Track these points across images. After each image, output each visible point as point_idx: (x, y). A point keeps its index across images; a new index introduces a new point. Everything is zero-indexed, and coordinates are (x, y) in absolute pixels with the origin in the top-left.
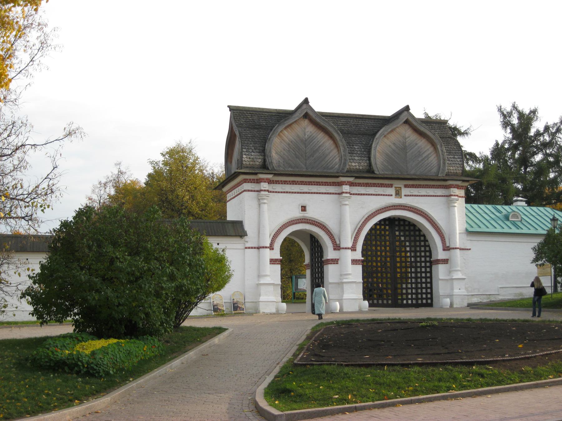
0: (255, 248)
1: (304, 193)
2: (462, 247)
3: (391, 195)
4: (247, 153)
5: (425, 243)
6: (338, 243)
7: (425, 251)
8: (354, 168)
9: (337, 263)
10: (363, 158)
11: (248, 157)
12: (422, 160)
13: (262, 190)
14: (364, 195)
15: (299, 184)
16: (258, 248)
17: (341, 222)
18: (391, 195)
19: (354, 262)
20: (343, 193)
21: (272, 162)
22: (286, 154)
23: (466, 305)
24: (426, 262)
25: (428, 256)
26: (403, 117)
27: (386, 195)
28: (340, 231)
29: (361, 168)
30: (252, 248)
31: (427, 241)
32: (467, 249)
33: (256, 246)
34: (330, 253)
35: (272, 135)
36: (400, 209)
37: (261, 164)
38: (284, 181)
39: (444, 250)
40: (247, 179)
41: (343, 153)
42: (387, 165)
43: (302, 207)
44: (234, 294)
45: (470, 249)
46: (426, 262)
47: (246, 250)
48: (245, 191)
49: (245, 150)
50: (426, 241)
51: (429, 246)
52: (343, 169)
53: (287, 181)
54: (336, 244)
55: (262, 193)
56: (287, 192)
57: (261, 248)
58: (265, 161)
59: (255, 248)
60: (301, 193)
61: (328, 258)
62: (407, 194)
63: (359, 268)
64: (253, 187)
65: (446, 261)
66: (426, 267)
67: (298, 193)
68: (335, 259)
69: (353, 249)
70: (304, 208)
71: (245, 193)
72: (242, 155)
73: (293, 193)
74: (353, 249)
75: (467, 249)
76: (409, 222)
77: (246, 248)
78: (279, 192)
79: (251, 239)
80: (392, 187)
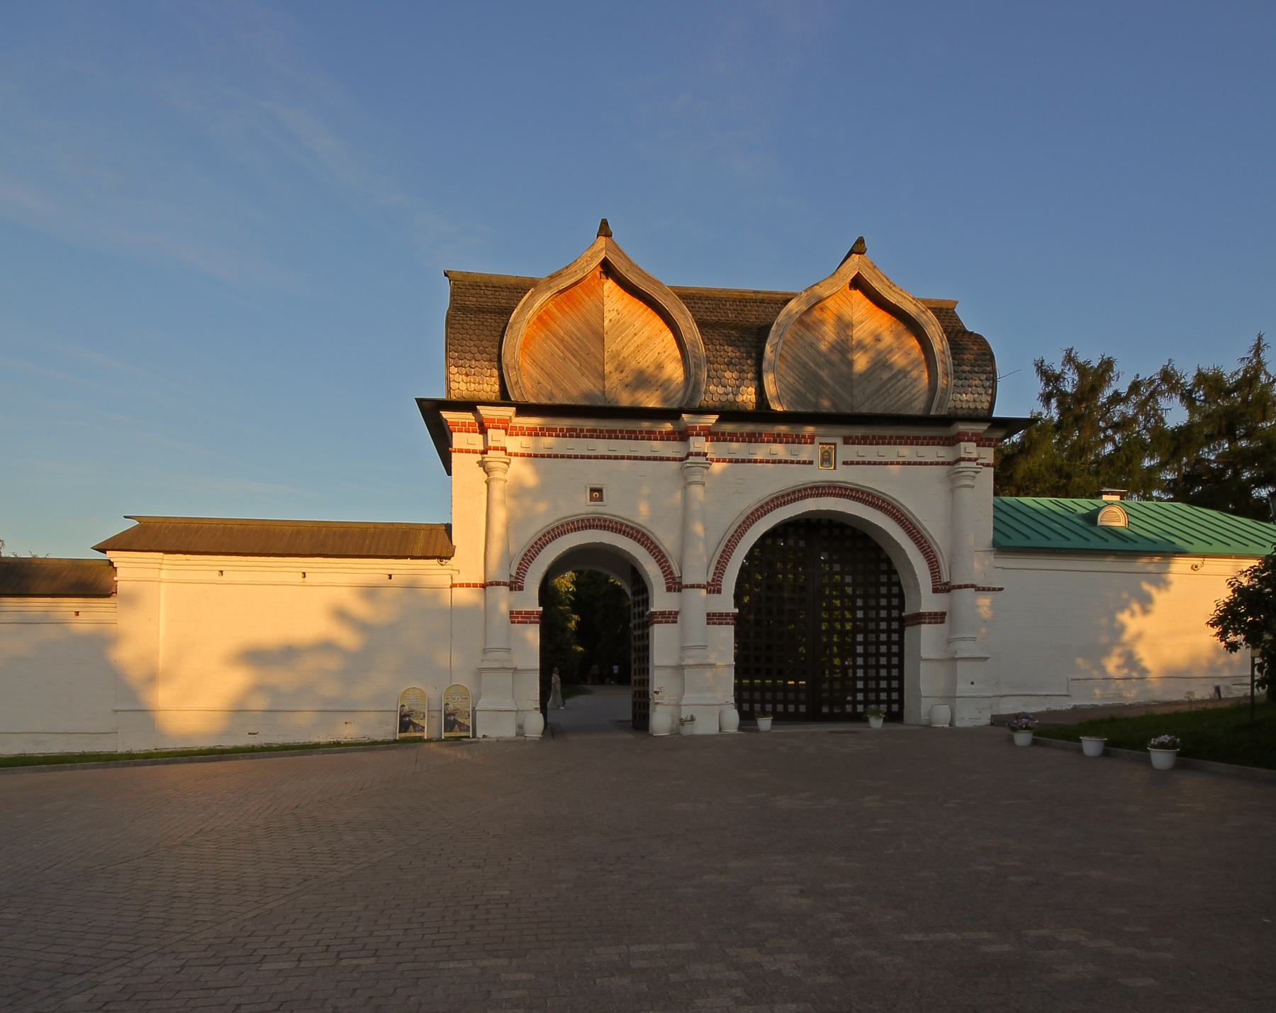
2: (981, 585)
3: (811, 463)
6: (677, 574)
7: (889, 596)
18: (811, 463)
19: (714, 618)
24: (889, 620)
25: (895, 607)
31: (895, 572)
32: (994, 589)
34: (661, 600)
39: (935, 591)
42: (803, 390)
43: (593, 490)
44: (404, 695)
46: (889, 620)
50: (892, 571)
54: (674, 579)
62: (849, 460)
63: (727, 634)
65: (938, 618)
66: (889, 631)
67: (583, 457)
68: (670, 613)
69: (714, 587)
70: (597, 493)
74: (714, 587)
75: (994, 589)
76: (854, 530)
80: (812, 443)
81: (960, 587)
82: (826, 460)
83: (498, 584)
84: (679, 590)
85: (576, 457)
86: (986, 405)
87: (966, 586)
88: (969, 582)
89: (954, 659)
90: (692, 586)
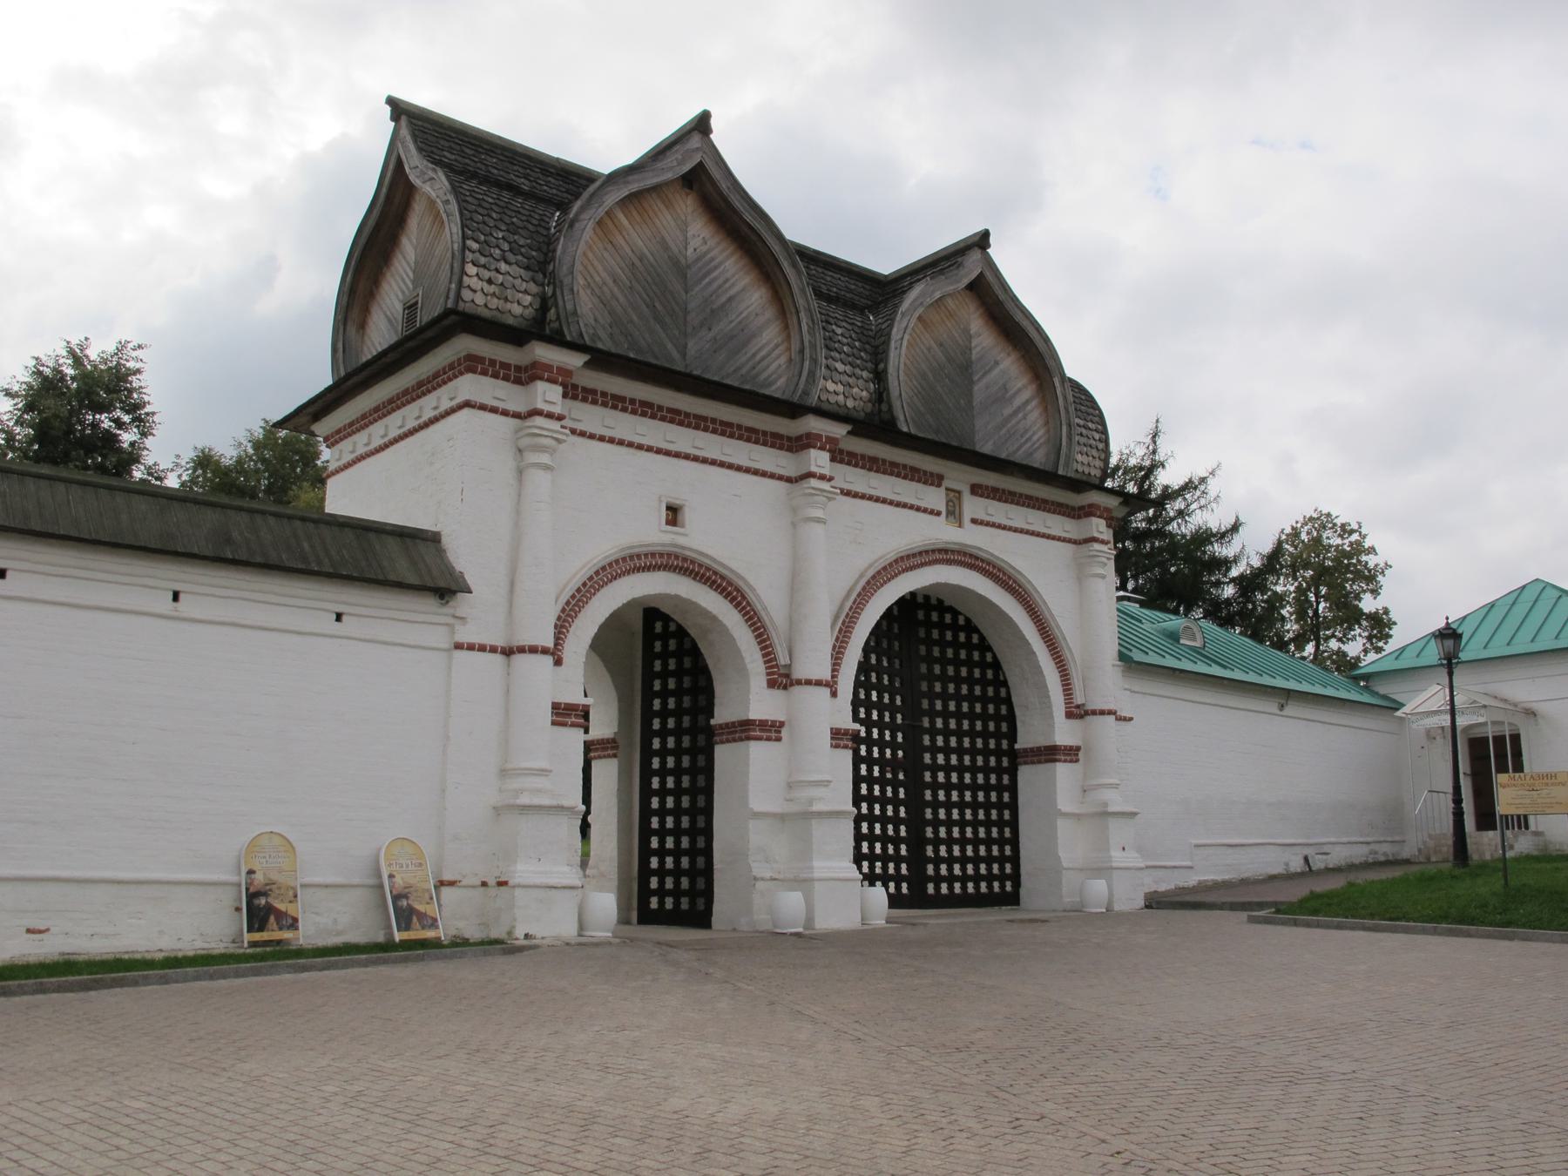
0: (493, 650)
1: (677, 455)
3: (938, 514)
4: (483, 260)
6: (783, 659)
8: (833, 399)
9: (779, 739)
10: (858, 371)
11: (486, 274)
12: (1016, 413)
14: (863, 497)
15: (663, 419)
16: (508, 652)
17: (796, 584)
21: (575, 313)
22: (622, 299)
23: (1142, 903)
26: (971, 268)
27: (925, 511)
28: (792, 622)
29: (850, 403)
30: (482, 648)
33: (500, 642)
35: (583, 209)
36: (949, 562)
37: (529, 312)
38: (614, 397)
39: (1069, 715)
40: (480, 360)
41: (807, 338)
47: (458, 654)
48: (467, 404)
49: (475, 246)
52: (806, 393)
55: (539, 421)
56: (621, 443)
57: (521, 650)
58: (544, 304)
59: (493, 650)
60: (668, 453)
61: (752, 716)
64: (500, 394)
67: (659, 451)
70: (674, 514)
71: (466, 411)
72: (463, 262)
73: (640, 447)
74: (831, 686)
77: (458, 646)
78: (592, 436)
79: (480, 614)
80: (939, 485)
81: (1094, 713)
82: (954, 513)
83: (533, 650)
84: (785, 688)
85: (649, 449)
86: (1098, 473)
87: (1102, 713)
88: (1106, 707)
89: (1105, 814)
90: (809, 682)
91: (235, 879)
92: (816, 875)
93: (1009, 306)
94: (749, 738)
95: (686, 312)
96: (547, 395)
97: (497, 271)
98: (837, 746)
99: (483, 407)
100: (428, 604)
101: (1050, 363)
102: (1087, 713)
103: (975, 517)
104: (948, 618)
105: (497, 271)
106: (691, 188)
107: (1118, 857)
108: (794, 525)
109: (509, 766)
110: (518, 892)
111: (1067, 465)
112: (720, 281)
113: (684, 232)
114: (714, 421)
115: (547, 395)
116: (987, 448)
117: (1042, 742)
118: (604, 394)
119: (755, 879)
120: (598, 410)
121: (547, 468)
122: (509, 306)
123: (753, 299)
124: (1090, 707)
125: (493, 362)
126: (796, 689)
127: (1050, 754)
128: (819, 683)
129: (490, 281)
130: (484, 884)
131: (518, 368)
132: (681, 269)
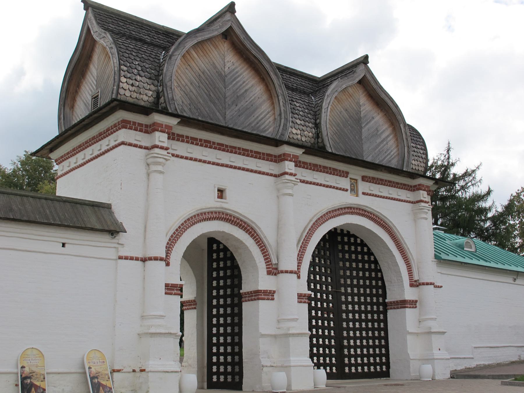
0: (137, 259)
1: (222, 165)
3: (347, 190)
4: (129, 75)
5: (376, 275)
6: (274, 261)
8: (295, 137)
9: (273, 299)
10: (307, 124)
11: (131, 82)
13: (156, 147)
14: (311, 183)
16: (144, 260)
18: (347, 190)
20: (285, 173)
21: (173, 99)
22: (194, 92)
23: (449, 376)
26: (360, 73)
27: (340, 189)
28: (278, 244)
29: (304, 139)
30: (132, 259)
33: (140, 256)
35: (175, 50)
36: (352, 213)
37: (151, 99)
38: (192, 138)
39: (411, 285)
40: (129, 122)
41: (282, 108)
45: (441, 287)
48: (123, 143)
49: (125, 68)
51: (382, 279)
52: (282, 134)
53: (196, 139)
55: (157, 150)
56: (196, 160)
57: (150, 259)
59: (137, 259)
60: (218, 164)
61: (260, 288)
70: (221, 193)
71: (122, 146)
72: (120, 76)
73: (205, 162)
74: (297, 273)
77: (120, 258)
78: (182, 157)
79: (130, 243)
80: (347, 177)
81: (423, 284)
82: (354, 190)
83: (156, 259)
84: (275, 275)
85: (209, 163)
86: (423, 169)
87: (427, 284)
88: (429, 281)
89: (430, 333)
90: (286, 272)
91: (15, 371)
92: (292, 364)
93: (379, 91)
94: (259, 299)
95: (225, 98)
96: (160, 138)
97: (136, 80)
98: (301, 302)
99: (130, 145)
100: (106, 238)
101: (399, 117)
102: (420, 284)
103: (365, 191)
104: (352, 240)
105: (136, 80)
106: (226, 39)
107: (437, 354)
108: (278, 197)
109: (145, 314)
110: (150, 374)
111: (408, 166)
112: (241, 83)
113: (223, 60)
114: (239, 149)
115: (160, 138)
116: (369, 159)
117: (399, 298)
118: (187, 137)
119: (263, 366)
120: (185, 145)
121: (161, 172)
122: (142, 96)
123: (256, 90)
124: (421, 281)
125: (134, 123)
126: (281, 275)
127: (403, 304)
128: (291, 272)
129: (132, 85)
130: (134, 371)
131: (146, 126)
132: (222, 77)
